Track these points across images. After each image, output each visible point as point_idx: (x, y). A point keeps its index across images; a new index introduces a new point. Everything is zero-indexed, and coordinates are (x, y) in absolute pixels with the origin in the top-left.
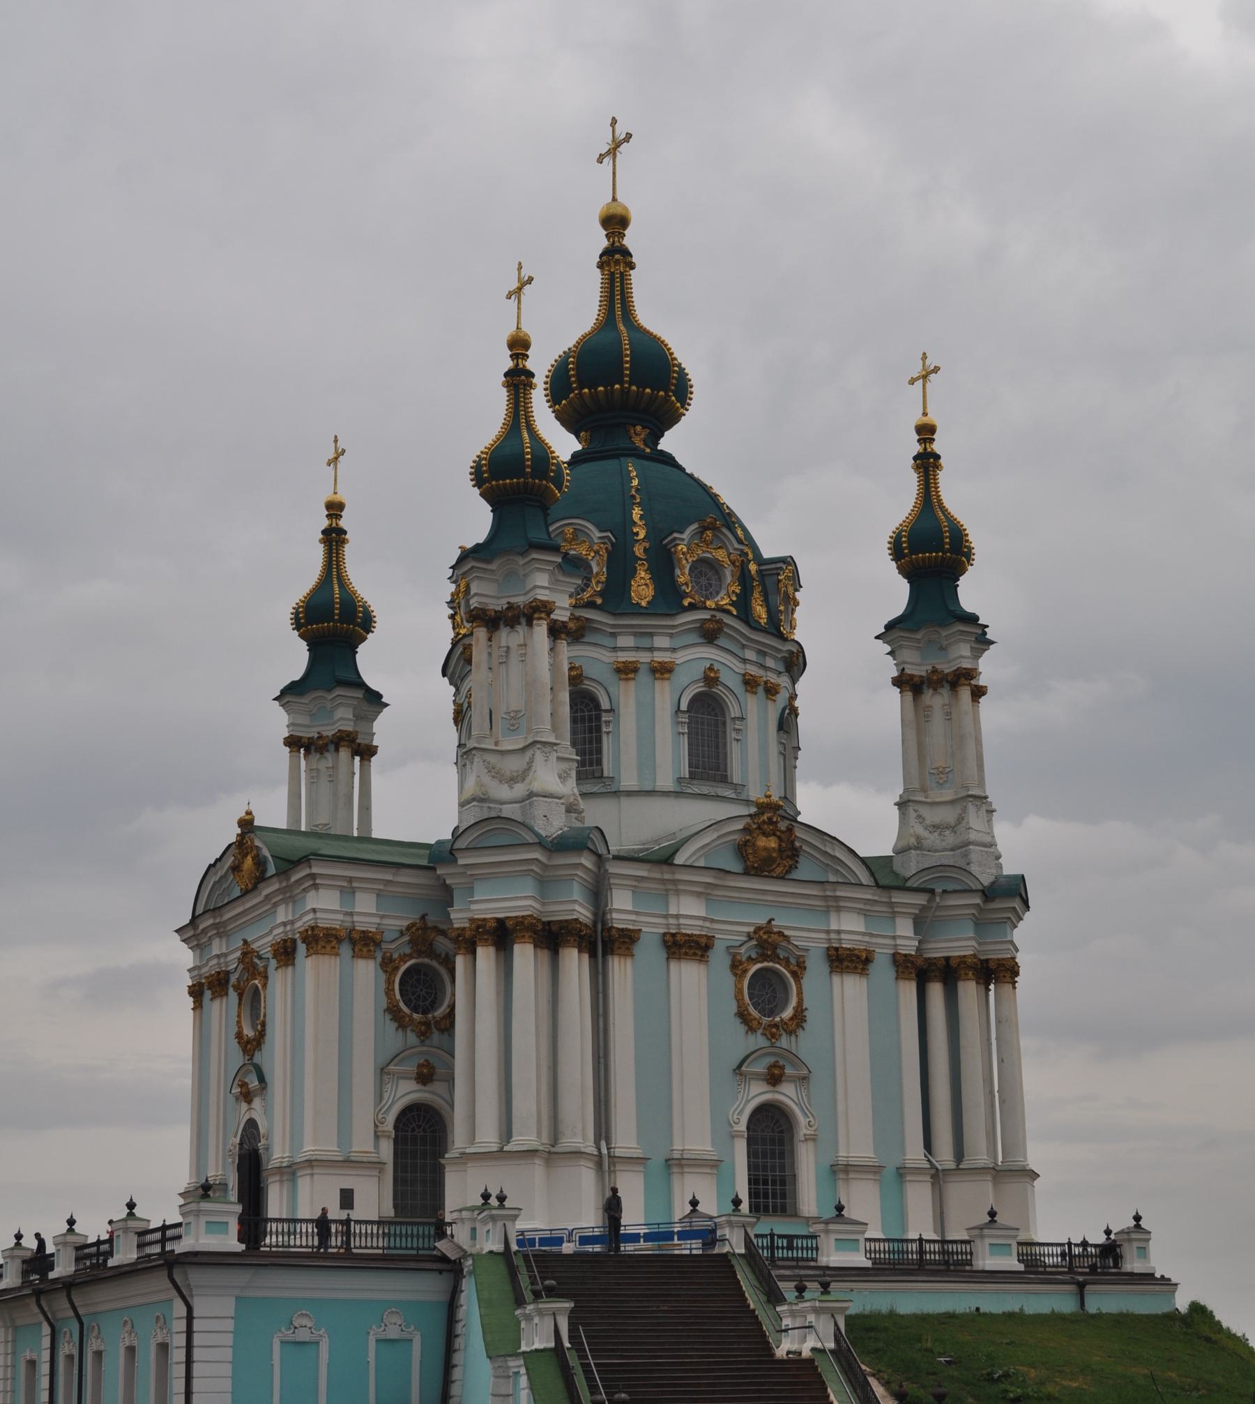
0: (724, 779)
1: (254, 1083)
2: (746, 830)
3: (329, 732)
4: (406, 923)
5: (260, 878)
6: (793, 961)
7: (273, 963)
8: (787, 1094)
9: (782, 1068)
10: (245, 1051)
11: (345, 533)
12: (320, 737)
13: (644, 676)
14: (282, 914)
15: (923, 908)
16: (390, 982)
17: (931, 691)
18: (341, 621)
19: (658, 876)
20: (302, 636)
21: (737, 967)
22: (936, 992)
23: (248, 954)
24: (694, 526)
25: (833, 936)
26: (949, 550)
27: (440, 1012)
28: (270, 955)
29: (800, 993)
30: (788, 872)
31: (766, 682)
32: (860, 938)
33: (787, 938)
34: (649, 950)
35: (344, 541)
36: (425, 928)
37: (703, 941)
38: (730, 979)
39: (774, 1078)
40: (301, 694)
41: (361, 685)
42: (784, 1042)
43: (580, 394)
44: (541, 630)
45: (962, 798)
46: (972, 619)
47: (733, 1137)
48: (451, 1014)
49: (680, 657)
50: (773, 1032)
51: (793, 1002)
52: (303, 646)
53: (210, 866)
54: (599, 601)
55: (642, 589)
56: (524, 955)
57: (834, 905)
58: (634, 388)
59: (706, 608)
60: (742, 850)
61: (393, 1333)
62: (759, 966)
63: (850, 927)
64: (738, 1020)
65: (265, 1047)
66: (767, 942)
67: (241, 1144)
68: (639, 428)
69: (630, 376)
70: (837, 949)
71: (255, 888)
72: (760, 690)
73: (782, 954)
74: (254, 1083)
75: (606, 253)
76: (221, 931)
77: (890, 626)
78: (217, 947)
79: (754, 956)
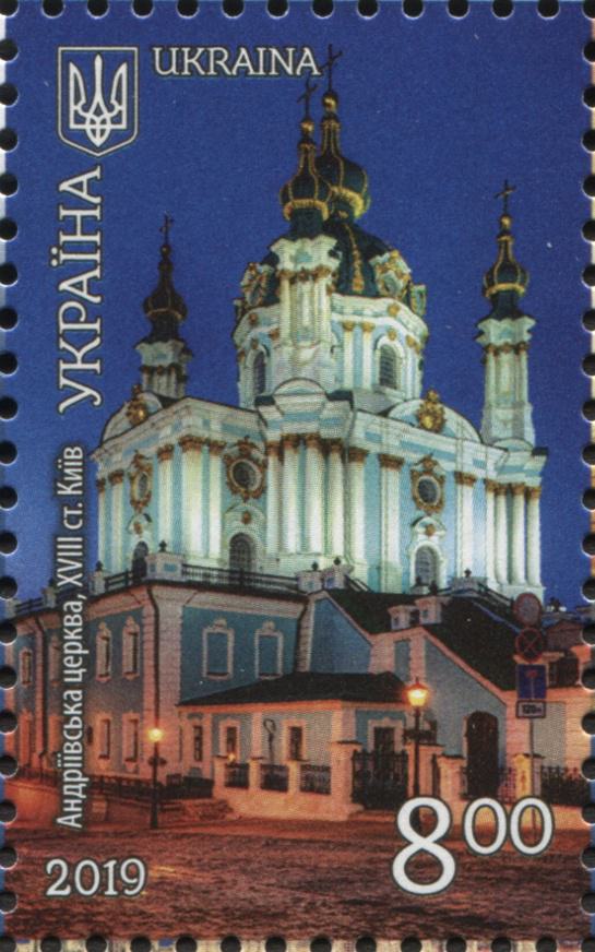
1: (144, 523)
2: (421, 406)
3: (166, 363)
4: (235, 440)
10: (136, 508)
12: (161, 367)
13: (357, 330)
16: (228, 467)
21: (414, 475)
23: (138, 458)
27: (255, 488)
34: (372, 461)
36: (246, 443)
48: (263, 490)
49: (378, 322)
51: (438, 497)
56: (313, 456)
60: (419, 417)
64: (413, 503)
65: (151, 505)
66: (428, 462)
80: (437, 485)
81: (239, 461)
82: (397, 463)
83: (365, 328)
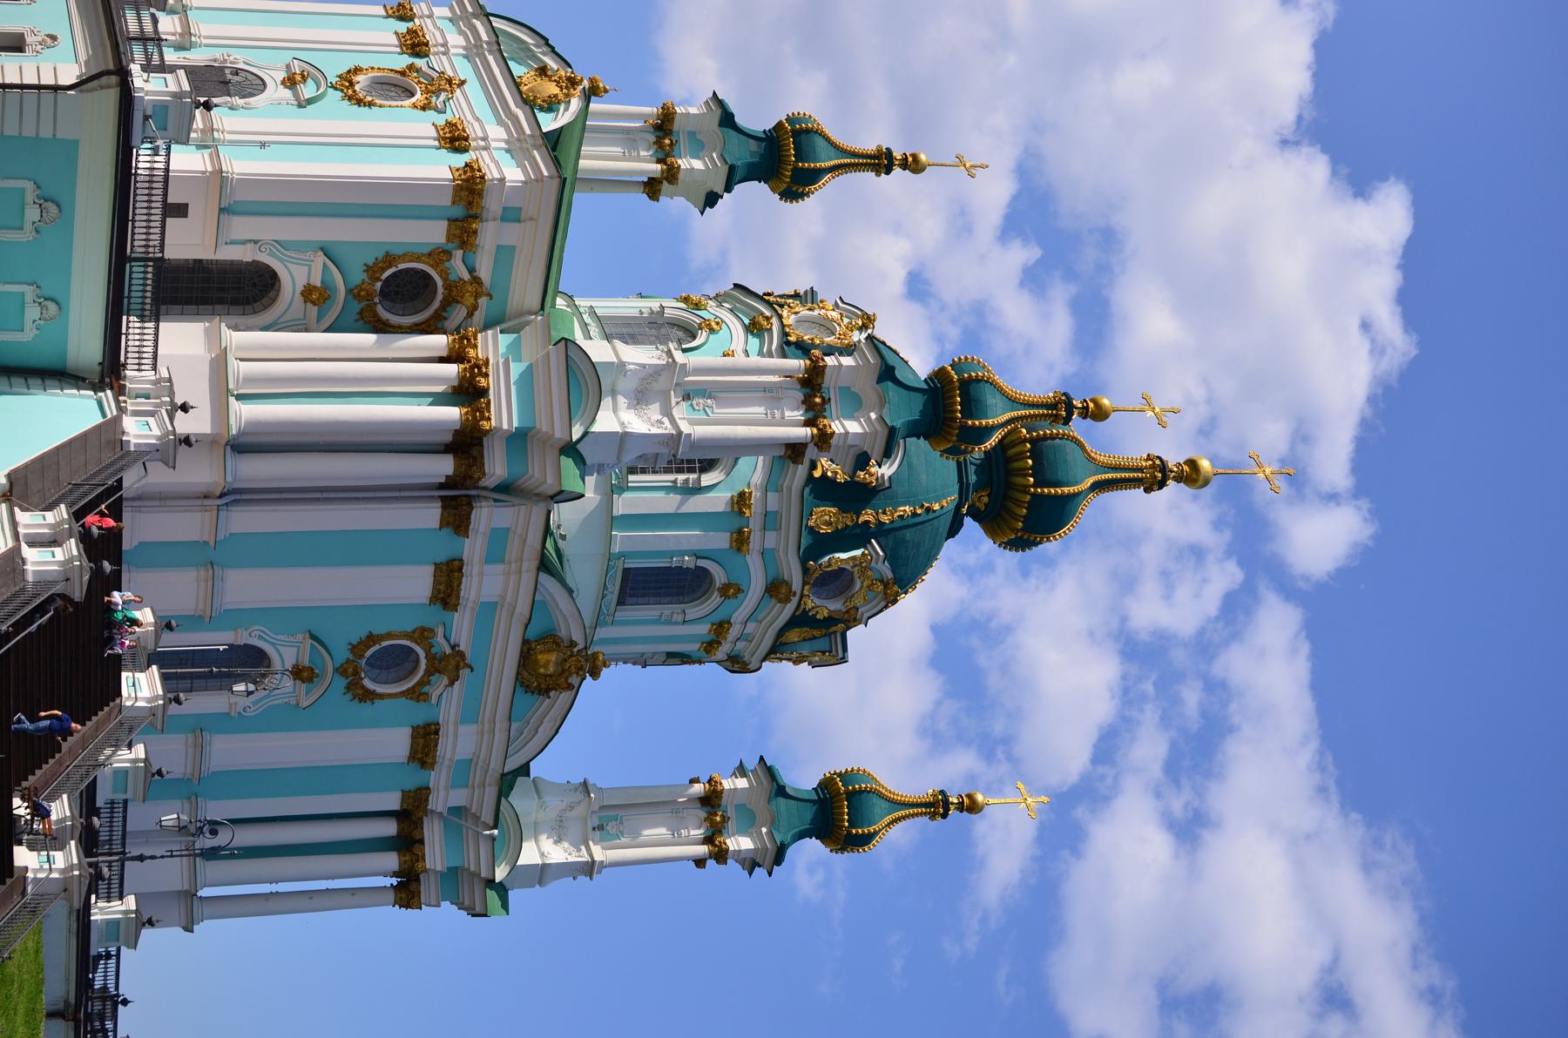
0: (621, 602)
2: (573, 644)
4: (484, 273)
5: (530, 103)
6: (426, 689)
7: (441, 120)
9: (310, 680)
11: (888, 173)
14: (496, 133)
15: (476, 818)
17: (703, 815)
18: (796, 170)
19: (526, 556)
20: (779, 125)
21: (423, 635)
24: (890, 575)
25: (451, 728)
26: (849, 833)
27: (380, 309)
28: (448, 116)
29: (390, 696)
30: (522, 684)
31: (719, 643)
32: (448, 756)
33: (452, 683)
35: (878, 174)
36: (477, 296)
37: (453, 601)
38: (410, 628)
39: (301, 673)
40: (721, 124)
41: (728, 189)
42: (342, 683)
43: (1025, 440)
44: (805, 432)
45: (591, 855)
46: (779, 856)
48: (380, 327)
49: (754, 561)
50: (350, 673)
52: (769, 125)
53: (546, 40)
54: (817, 474)
55: (825, 517)
58: (1028, 498)
59: (805, 583)
60: (551, 639)
61: (32, 312)
62: (422, 654)
63: (457, 743)
64: (364, 635)
67: (236, 72)
68: (986, 499)
69: (1042, 495)
70: (437, 732)
71: (525, 101)
72: (712, 636)
74: (308, 90)
75: (1163, 467)
76: (473, 52)
77: (770, 772)
78: (455, 40)
79: (433, 650)
80: (410, 685)
81: (439, 282)
83: (740, 541)
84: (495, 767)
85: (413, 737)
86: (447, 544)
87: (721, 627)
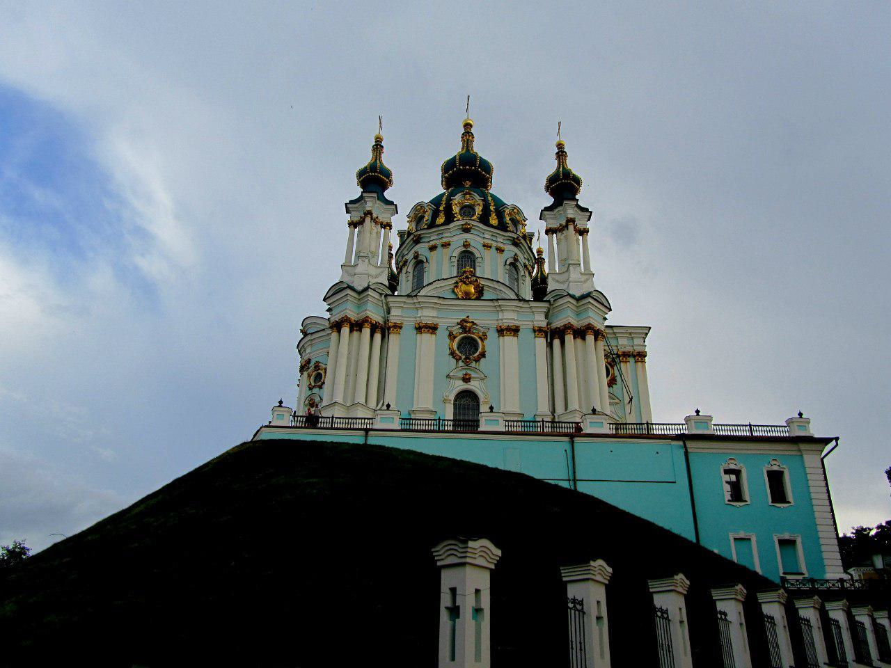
2: (457, 283)
8: (474, 386)
19: (412, 302)
21: (452, 336)
22: (557, 342)
33: (475, 324)
38: (448, 341)
39: (466, 379)
42: (473, 364)
47: (445, 401)
50: (467, 361)
51: (480, 350)
54: (426, 227)
57: (500, 309)
63: (509, 317)
70: (500, 327)
72: (493, 250)
73: (474, 331)
82: (433, 329)
83: (446, 245)
84: (516, 303)
85: (503, 336)
86: (408, 330)
87: (487, 246)
